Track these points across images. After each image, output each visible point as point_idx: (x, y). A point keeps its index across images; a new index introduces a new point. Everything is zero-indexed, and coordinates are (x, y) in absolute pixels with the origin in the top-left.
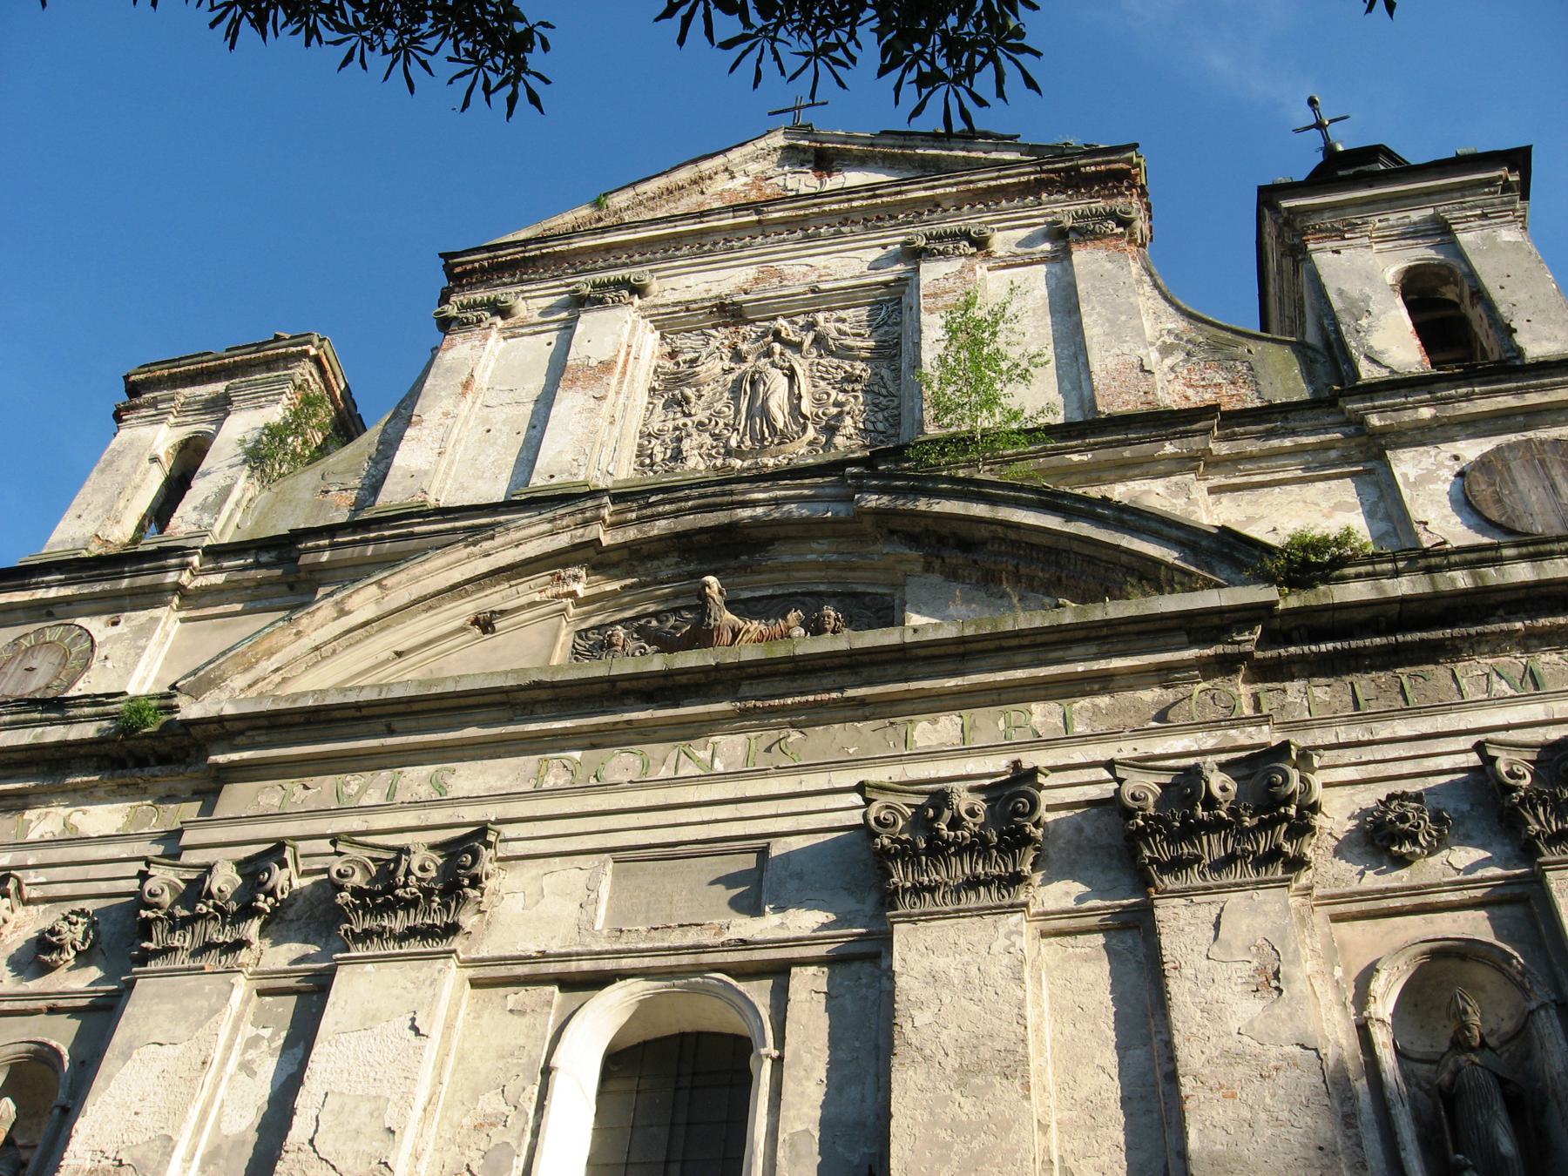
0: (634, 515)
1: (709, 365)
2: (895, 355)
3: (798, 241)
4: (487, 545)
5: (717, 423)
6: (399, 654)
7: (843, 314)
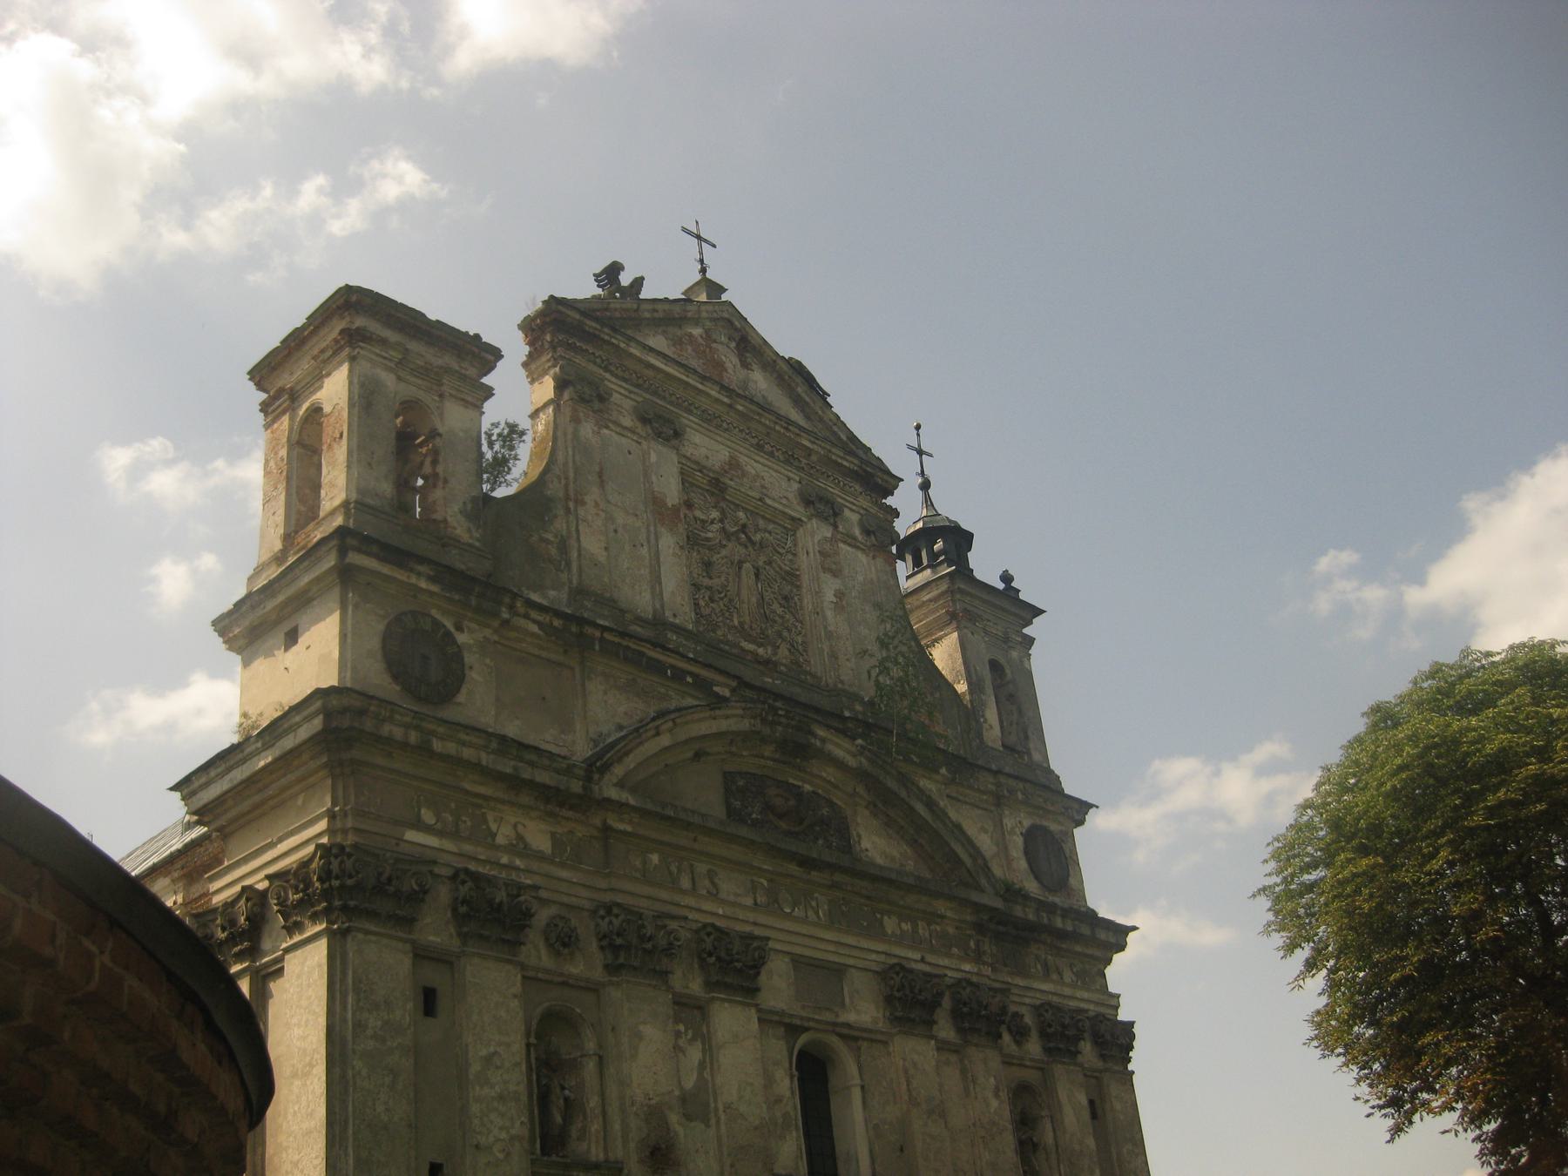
3: (752, 445)
4: (718, 712)
5: (726, 596)
6: (666, 765)
7: (771, 527)
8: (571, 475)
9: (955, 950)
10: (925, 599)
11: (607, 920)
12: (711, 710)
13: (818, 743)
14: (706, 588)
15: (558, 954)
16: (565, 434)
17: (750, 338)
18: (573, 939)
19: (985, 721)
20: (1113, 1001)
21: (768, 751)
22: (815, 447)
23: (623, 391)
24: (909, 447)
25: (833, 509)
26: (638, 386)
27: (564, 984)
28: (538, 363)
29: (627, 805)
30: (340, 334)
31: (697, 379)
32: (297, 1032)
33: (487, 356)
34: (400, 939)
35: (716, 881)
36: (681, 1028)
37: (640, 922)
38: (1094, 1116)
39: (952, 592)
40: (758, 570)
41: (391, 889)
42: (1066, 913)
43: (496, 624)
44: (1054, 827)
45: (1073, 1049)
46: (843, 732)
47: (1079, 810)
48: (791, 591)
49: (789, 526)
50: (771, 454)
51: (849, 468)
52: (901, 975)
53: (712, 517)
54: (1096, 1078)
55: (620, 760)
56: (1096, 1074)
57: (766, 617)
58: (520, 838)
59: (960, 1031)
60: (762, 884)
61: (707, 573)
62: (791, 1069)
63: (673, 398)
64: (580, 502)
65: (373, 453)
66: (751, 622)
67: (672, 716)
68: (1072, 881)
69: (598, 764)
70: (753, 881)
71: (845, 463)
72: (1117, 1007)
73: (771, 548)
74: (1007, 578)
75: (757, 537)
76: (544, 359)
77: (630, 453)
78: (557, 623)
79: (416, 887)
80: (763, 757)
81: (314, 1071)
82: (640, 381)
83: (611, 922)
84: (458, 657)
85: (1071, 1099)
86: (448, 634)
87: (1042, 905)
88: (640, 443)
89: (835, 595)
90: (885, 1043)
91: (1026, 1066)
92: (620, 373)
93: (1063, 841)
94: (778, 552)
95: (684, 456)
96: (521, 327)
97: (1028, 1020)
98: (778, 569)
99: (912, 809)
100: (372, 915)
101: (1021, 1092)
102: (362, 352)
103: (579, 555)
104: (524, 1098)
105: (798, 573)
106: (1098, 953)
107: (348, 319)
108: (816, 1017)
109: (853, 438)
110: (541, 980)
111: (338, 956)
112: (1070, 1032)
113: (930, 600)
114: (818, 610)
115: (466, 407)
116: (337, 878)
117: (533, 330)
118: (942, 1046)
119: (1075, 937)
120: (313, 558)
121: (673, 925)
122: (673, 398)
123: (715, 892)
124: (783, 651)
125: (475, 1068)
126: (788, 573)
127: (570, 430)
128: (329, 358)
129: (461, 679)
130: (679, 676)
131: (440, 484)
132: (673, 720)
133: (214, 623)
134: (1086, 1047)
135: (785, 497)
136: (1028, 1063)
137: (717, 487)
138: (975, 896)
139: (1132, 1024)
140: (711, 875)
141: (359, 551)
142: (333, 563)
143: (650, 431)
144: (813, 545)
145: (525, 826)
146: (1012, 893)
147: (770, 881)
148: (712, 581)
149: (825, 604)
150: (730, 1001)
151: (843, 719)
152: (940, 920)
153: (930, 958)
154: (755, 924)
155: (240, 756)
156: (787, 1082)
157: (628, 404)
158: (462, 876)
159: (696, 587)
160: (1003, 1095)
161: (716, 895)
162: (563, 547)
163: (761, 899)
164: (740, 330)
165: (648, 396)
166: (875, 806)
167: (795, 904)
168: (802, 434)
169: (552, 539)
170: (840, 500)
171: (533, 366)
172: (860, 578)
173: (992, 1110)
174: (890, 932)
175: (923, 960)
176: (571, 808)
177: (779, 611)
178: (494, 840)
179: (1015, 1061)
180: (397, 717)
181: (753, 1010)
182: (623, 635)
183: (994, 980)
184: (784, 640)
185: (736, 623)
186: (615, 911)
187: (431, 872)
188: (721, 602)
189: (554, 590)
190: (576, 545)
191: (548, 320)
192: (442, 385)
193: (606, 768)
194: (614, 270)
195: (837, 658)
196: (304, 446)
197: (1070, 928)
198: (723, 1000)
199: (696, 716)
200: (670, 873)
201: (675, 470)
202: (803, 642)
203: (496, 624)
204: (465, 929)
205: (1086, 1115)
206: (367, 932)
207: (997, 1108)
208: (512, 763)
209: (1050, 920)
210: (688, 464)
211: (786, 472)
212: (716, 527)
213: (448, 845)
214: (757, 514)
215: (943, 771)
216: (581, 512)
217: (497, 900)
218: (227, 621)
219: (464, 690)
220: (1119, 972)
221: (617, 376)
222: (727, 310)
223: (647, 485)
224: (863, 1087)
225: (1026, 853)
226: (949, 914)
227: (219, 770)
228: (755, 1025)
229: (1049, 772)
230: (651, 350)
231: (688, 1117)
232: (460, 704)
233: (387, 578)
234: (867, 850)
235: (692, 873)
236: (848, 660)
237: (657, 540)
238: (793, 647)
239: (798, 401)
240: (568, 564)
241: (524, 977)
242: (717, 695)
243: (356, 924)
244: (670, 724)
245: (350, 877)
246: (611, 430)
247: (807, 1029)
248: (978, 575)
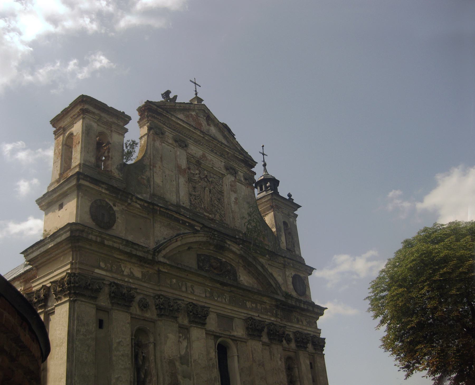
0: (213, 237)
3: (210, 150)
5: (200, 198)
7: (215, 176)
8: (152, 157)
9: (269, 313)
10: (263, 201)
11: (158, 300)
12: (194, 234)
13: (228, 246)
15: (142, 310)
16: (150, 145)
17: (210, 116)
18: (147, 306)
19: (281, 241)
20: (319, 331)
21: (212, 248)
22: (230, 151)
23: (169, 131)
24: (260, 153)
25: (235, 171)
26: (174, 130)
27: (144, 320)
28: (143, 122)
29: (166, 263)
30: (80, 110)
31: (193, 129)
32: (58, 332)
33: (126, 119)
34: (92, 304)
35: (194, 288)
36: (181, 335)
37: (169, 301)
38: (311, 368)
39: (272, 199)
40: (210, 190)
41: (90, 288)
42: (305, 303)
43: (126, 204)
44: (302, 275)
45: (305, 346)
46: (236, 243)
47: (310, 270)
48: (221, 197)
49: (221, 177)
50: (216, 153)
51: (241, 159)
52: (251, 321)
53: (196, 172)
54: (312, 355)
55: (164, 249)
56: (312, 354)
58: (132, 273)
59: (270, 339)
60: (208, 290)
62: (215, 349)
63: (185, 135)
64: (154, 166)
65: (89, 148)
66: (208, 206)
67: (182, 236)
68: (307, 293)
69: (157, 250)
70: (205, 289)
71: (239, 157)
72: (320, 333)
74: (290, 195)
75: (210, 180)
76: (145, 120)
77: (171, 151)
78: (146, 205)
79: (98, 287)
80: (210, 250)
81: (63, 345)
82: (175, 129)
83: (159, 301)
84: (114, 214)
85: (304, 362)
86: (111, 207)
87: (297, 300)
88: (174, 148)
89: (235, 199)
90: (246, 342)
91: (290, 351)
92: (168, 126)
93: (305, 280)
94: (217, 185)
95: (188, 153)
96: (137, 110)
97: (292, 336)
98: (217, 190)
99: (257, 268)
100: (83, 296)
101: (288, 359)
102: (87, 116)
103: (154, 183)
104: (130, 356)
105: (223, 191)
106: (314, 316)
107: (82, 106)
108: (224, 333)
109: (242, 149)
110: (136, 318)
111: (72, 308)
112: (305, 341)
113: (265, 202)
114: (229, 203)
115: (119, 135)
116: (73, 283)
117: (141, 111)
118: (264, 344)
119: (307, 310)
120: (69, 181)
121: (179, 302)
122: (185, 135)
123: (193, 292)
124: (218, 216)
125: (115, 345)
126: (219, 191)
127: (152, 143)
128: (76, 118)
129: (115, 221)
130: (184, 223)
131: (110, 159)
132: (182, 237)
133: (36, 201)
134: (310, 346)
135: (220, 167)
136: (291, 350)
137: (198, 163)
138: (276, 296)
139: (324, 339)
140: (192, 287)
141: (83, 179)
142: (75, 183)
143: (177, 145)
144: (228, 182)
145: (133, 269)
146: (288, 296)
147: (211, 289)
148: (195, 193)
149: (231, 202)
150: (197, 327)
151: (236, 239)
152: (264, 304)
153: (261, 316)
154: (205, 303)
155: (43, 244)
156: (214, 353)
157: (171, 136)
158: (113, 284)
159: (191, 195)
160: (283, 360)
161: (193, 293)
162: (149, 180)
163: (208, 295)
164: (207, 114)
165: (177, 134)
166: (245, 266)
167: (218, 297)
168: (226, 147)
169: (145, 178)
170: (237, 169)
171: (141, 123)
172: (243, 194)
173: (279, 365)
174: (248, 307)
175: (259, 316)
176: (148, 264)
177: (217, 203)
178: (123, 273)
179: (287, 349)
180: (94, 233)
181: (204, 330)
182: (167, 209)
183: (281, 323)
184: (218, 212)
185: (203, 206)
186: (161, 297)
187: (103, 283)
189: (145, 194)
190: (153, 180)
191: (146, 108)
192: (112, 128)
193: (159, 252)
194: (168, 93)
195: (235, 219)
196: (67, 146)
197: (306, 308)
198: (195, 327)
199: (189, 236)
200: (179, 286)
201: (185, 157)
202: (224, 214)
203: (126, 204)
204: (113, 301)
205: (309, 367)
206: (82, 301)
207: (281, 364)
208: (130, 249)
209: (299, 304)
210: (189, 156)
211: (220, 159)
212: (198, 176)
213: (108, 274)
214: (211, 172)
215: (267, 256)
216: (155, 169)
217: (124, 292)
218: (41, 200)
219: (115, 225)
220: (321, 322)
221: (167, 127)
222: (204, 107)
223: (176, 162)
224: (238, 356)
225: (293, 283)
226: (267, 302)
227: (36, 248)
228: (204, 335)
229: (301, 258)
230: (179, 119)
231: (182, 363)
232: (114, 229)
233: (92, 189)
234: (242, 280)
235: (186, 286)
236: (238, 220)
237: (178, 179)
238: (221, 215)
239: (225, 137)
240: (150, 186)
241: (131, 317)
242: (196, 229)
243: (78, 299)
244: (181, 238)
245: (77, 283)
246: (165, 144)
247: (221, 337)
248: (281, 194)
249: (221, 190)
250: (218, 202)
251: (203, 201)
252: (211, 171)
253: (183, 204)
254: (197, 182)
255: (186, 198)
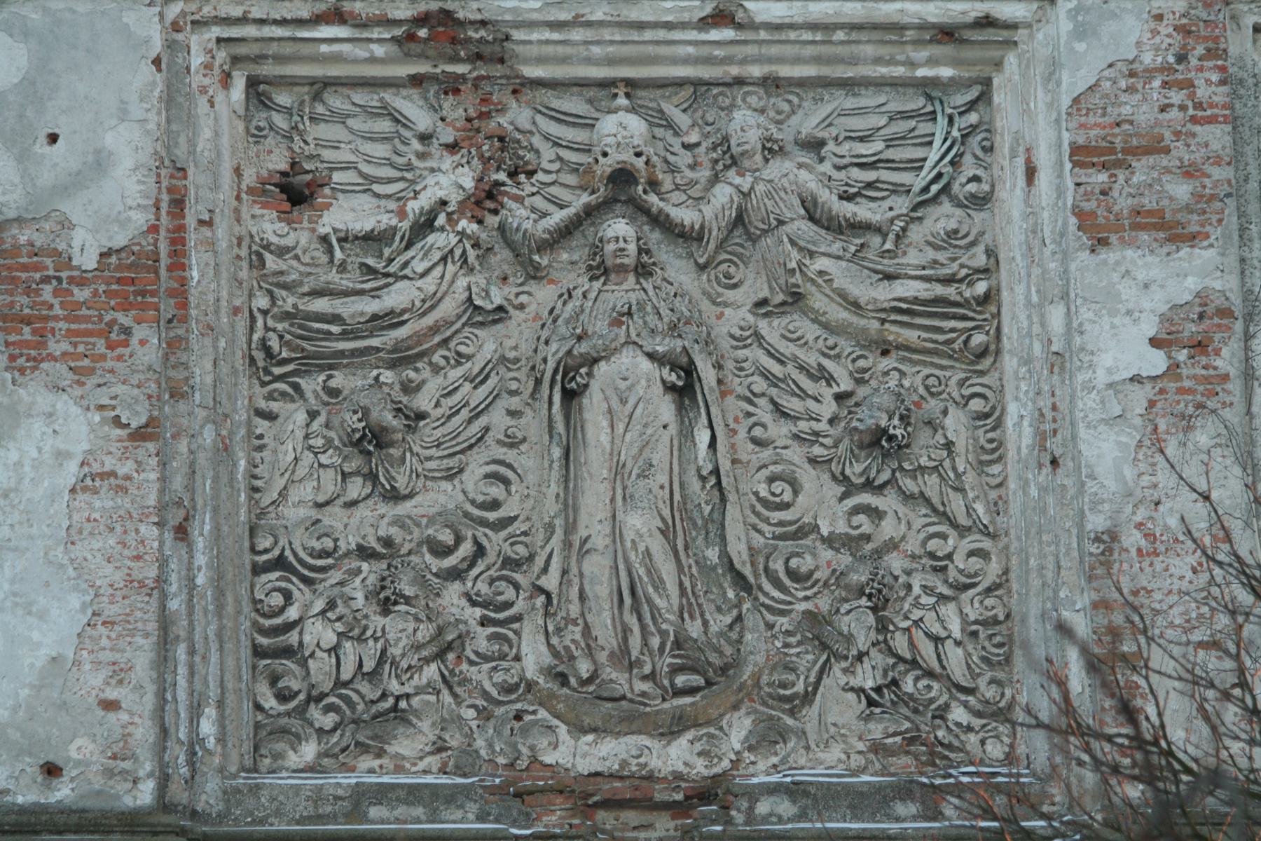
1: (429, 284)
2: (982, 353)
5: (480, 551)
14: (364, 553)
57: (740, 580)
61: (372, 477)
73: (803, 228)
98: (839, 314)
126: (907, 310)
188: (454, 591)
214: (740, 82)
249: (948, 281)
250: (869, 485)
251: (551, 582)
252: (735, 71)
253: (52, 770)
254: (434, 329)
255: (119, 674)
